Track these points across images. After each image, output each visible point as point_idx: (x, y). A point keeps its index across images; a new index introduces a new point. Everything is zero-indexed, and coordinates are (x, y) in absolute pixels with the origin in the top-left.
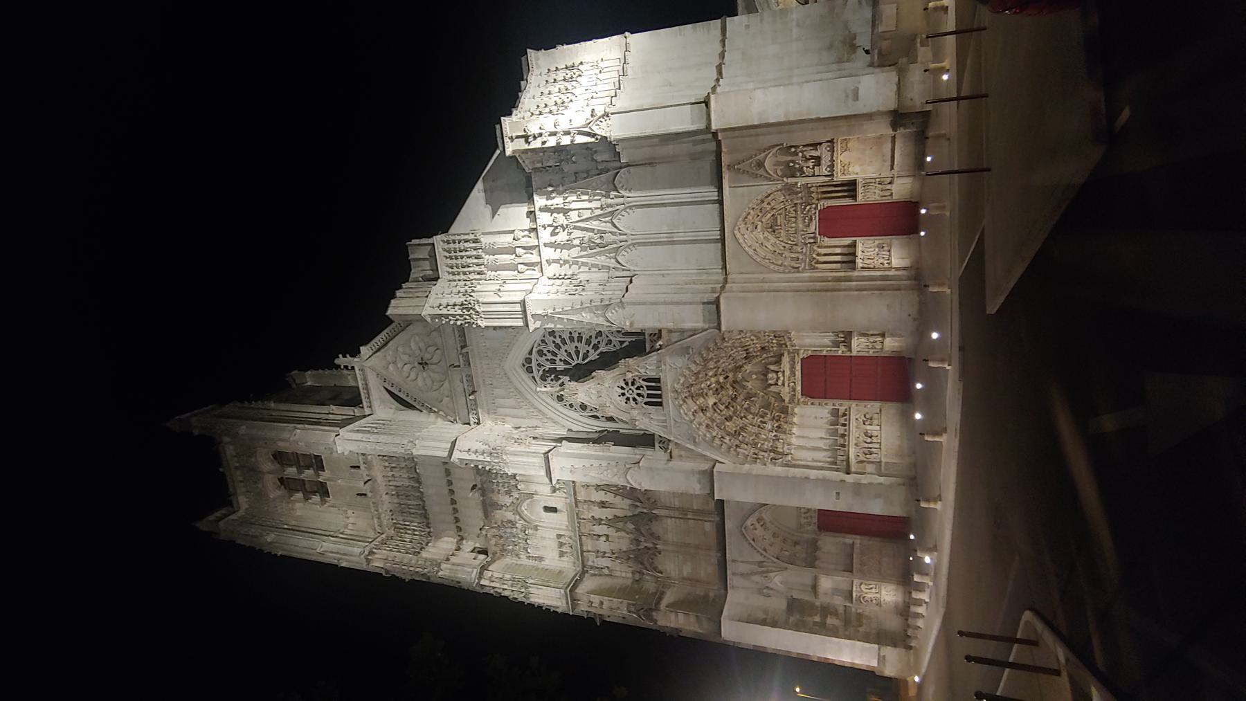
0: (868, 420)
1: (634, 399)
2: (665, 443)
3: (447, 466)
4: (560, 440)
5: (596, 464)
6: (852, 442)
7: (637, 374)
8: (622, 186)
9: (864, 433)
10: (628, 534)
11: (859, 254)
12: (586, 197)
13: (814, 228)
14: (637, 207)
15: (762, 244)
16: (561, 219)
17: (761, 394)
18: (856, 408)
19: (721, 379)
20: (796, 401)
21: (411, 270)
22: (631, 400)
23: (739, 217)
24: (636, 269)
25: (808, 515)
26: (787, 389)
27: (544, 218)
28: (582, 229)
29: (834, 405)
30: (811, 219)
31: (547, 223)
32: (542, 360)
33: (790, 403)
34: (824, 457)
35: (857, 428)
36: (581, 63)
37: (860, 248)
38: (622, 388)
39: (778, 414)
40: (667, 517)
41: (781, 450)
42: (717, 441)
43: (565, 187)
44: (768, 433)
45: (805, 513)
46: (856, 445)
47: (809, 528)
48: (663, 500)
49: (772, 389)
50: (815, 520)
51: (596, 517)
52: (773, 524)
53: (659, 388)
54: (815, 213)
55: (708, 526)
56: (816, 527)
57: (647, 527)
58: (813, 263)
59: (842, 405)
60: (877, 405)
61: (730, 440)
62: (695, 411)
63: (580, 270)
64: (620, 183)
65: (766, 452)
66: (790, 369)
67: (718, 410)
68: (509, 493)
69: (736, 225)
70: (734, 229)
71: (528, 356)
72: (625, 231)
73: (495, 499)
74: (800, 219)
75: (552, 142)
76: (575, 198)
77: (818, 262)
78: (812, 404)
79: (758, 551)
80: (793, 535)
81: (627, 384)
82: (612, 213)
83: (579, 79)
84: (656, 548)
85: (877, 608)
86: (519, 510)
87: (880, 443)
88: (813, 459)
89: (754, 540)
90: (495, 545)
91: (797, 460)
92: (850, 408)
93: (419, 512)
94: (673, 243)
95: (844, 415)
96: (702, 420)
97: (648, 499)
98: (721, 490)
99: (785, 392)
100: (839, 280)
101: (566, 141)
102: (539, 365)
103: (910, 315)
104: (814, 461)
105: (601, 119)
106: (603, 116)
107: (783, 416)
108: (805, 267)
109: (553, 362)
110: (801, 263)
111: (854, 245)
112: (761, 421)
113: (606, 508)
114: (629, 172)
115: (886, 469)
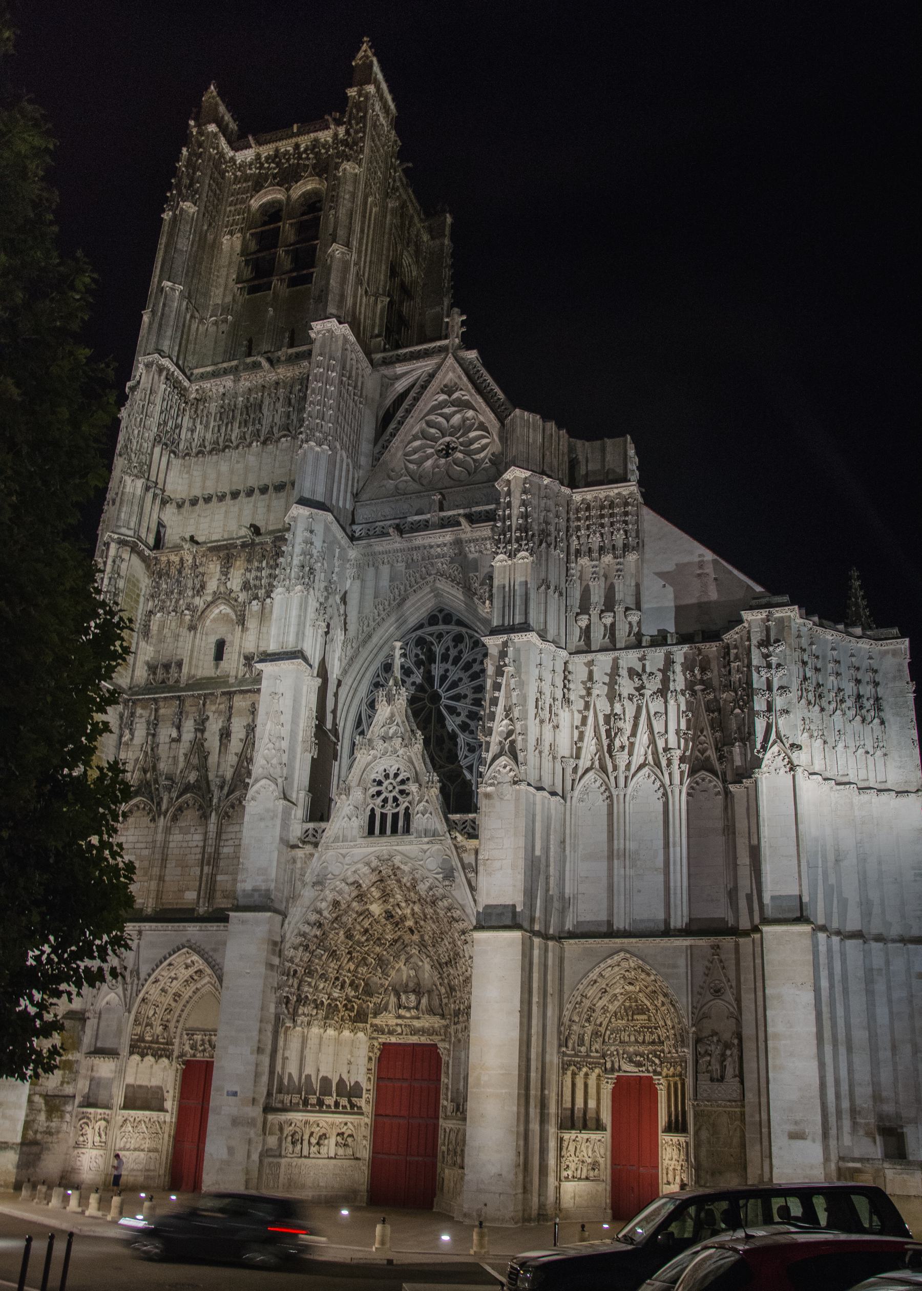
0: (344, 1139)
1: (379, 793)
2: (312, 840)
3: (288, 487)
4: (323, 673)
5: (285, 732)
6: (312, 1117)
7: (417, 798)
8: (697, 783)
9: (325, 1135)
10: (181, 772)
11: (584, 1135)
12: (683, 726)
13: (628, 1070)
14: (666, 805)
15: (606, 991)
16: (653, 685)
17: (387, 983)
18: (363, 1124)
19: (410, 923)
20: (375, 1035)
21: (588, 441)
22: (379, 788)
23: (642, 960)
24: (574, 799)
25: (207, 1046)
26: (393, 1022)
27: (656, 657)
28: (637, 718)
29: (368, 1090)
30: (639, 1064)
31: (647, 663)
32: (448, 640)
33: (372, 1025)
34: (290, 1075)
35: (333, 1124)
36: (882, 723)
37: (595, 1136)
38: (396, 775)
39: (356, 1007)
40: (206, 833)
41: (300, 1011)
42: (313, 917)
43: (699, 693)
44: (325, 991)
45: (210, 1041)
46: (306, 1122)
47: (187, 1048)
48: (230, 829)
49: (393, 999)
50: (199, 1057)
51: (207, 724)
52: (194, 992)
53: (394, 831)
54: (648, 1071)
55: (191, 896)
56: (188, 1058)
57: (191, 803)
58: (572, 1068)
59: (366, 1103)
60: (365, 1153)
61: (316, 936)
62: (360, 885)
63: (576, 713)
64: (703, 780)
65: (298, 989)
66: (423, 1027)
67: (362, 918)
68: (246, 586)
69: (633, 954)
70: (627, 951)
71: (454, 619)
72: (632, 784)
73: (238, 563)
74: (641, 1049)
75: (758, 682)
76: (683, 707)
77: (574, 1074)
78: (370, 1059)
79: (153, 970)
80: (178, 1021)
81: (403, 782)
82: (658, 764)
83: (858, 718)
84: (159, 817)
85: (71, 1142)
86: (220, 601)
87: (309, 1157)
88: (287, 1058)
89: (170, 964)
90: (169, 562)
91: (285, 1033)
92: (362, 1114)
93: (221, 440)
94: (611, 857)
95: (352, 1106)
96: (346, 896)
97: (233, 806)
98: (243, 922)
99: (387, 1019)
100: (543, 1105)
101: (759, 704)
102: (440, 636)
103: (486, 1205)
104: (285, 1059)
105: (787, 760)
106: (790, 762)
107: (352, 1014)
108: (569, 1056)
109: (445, 658)
110: (573, 1049)
111: (599, 1127)
112: (344, 982)
113: (221, 740)
114: (718, 793)
115: (270, 1164)
